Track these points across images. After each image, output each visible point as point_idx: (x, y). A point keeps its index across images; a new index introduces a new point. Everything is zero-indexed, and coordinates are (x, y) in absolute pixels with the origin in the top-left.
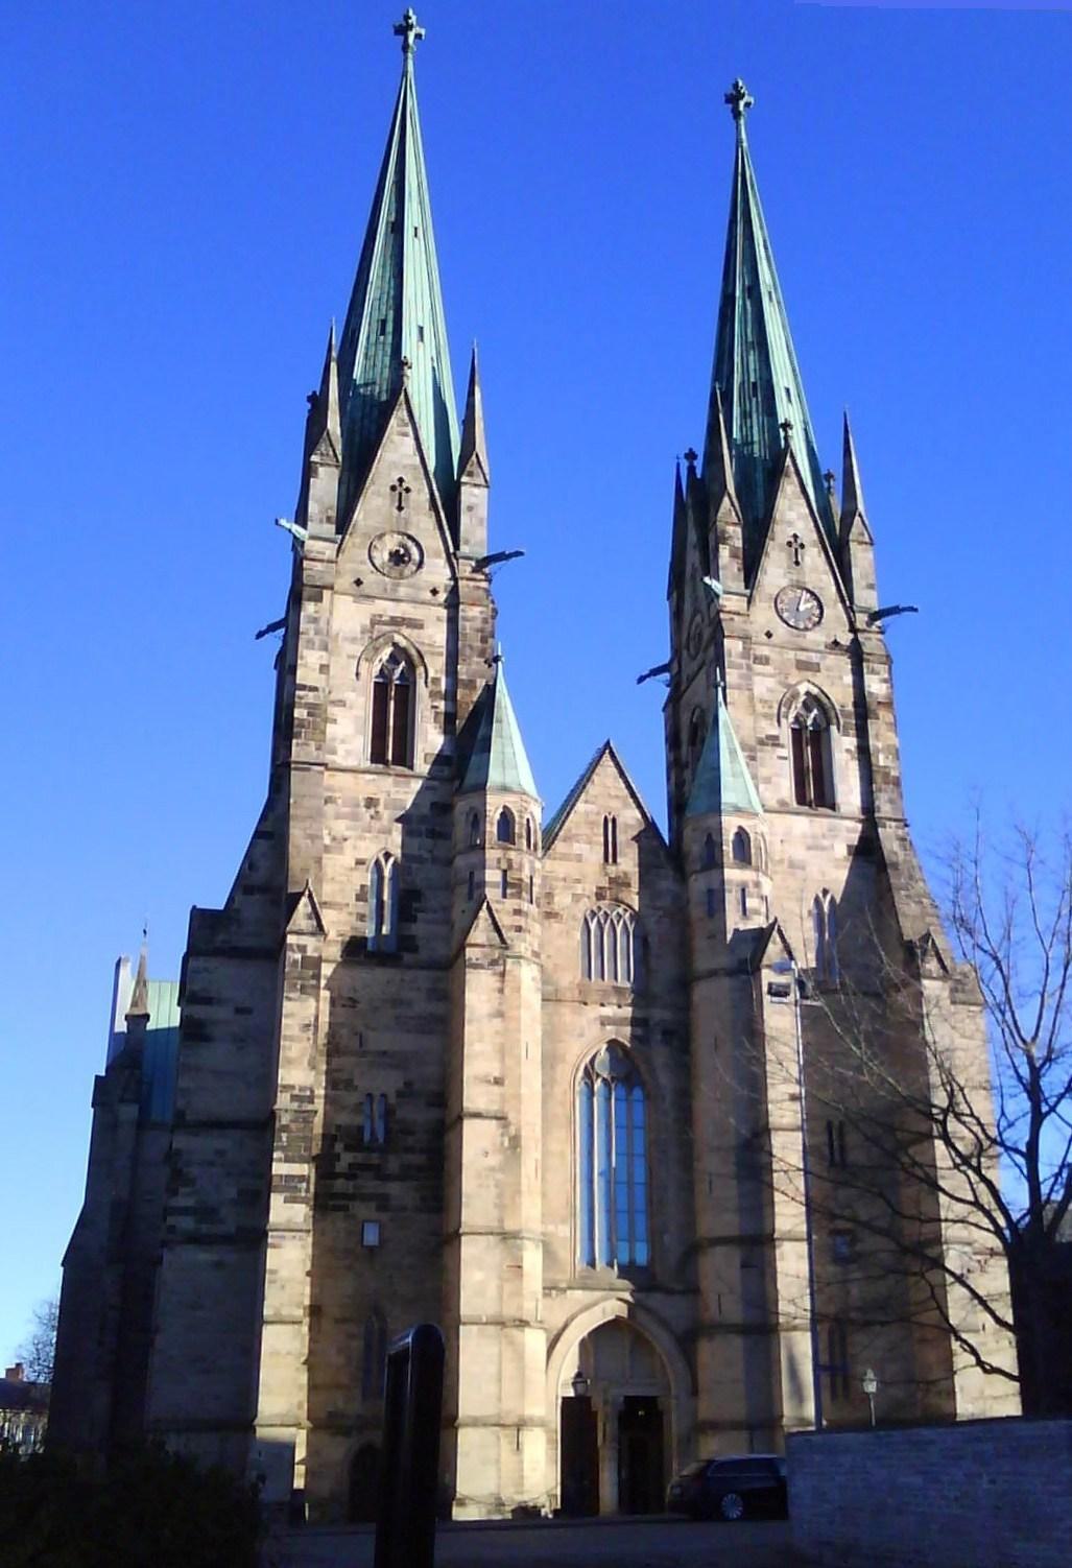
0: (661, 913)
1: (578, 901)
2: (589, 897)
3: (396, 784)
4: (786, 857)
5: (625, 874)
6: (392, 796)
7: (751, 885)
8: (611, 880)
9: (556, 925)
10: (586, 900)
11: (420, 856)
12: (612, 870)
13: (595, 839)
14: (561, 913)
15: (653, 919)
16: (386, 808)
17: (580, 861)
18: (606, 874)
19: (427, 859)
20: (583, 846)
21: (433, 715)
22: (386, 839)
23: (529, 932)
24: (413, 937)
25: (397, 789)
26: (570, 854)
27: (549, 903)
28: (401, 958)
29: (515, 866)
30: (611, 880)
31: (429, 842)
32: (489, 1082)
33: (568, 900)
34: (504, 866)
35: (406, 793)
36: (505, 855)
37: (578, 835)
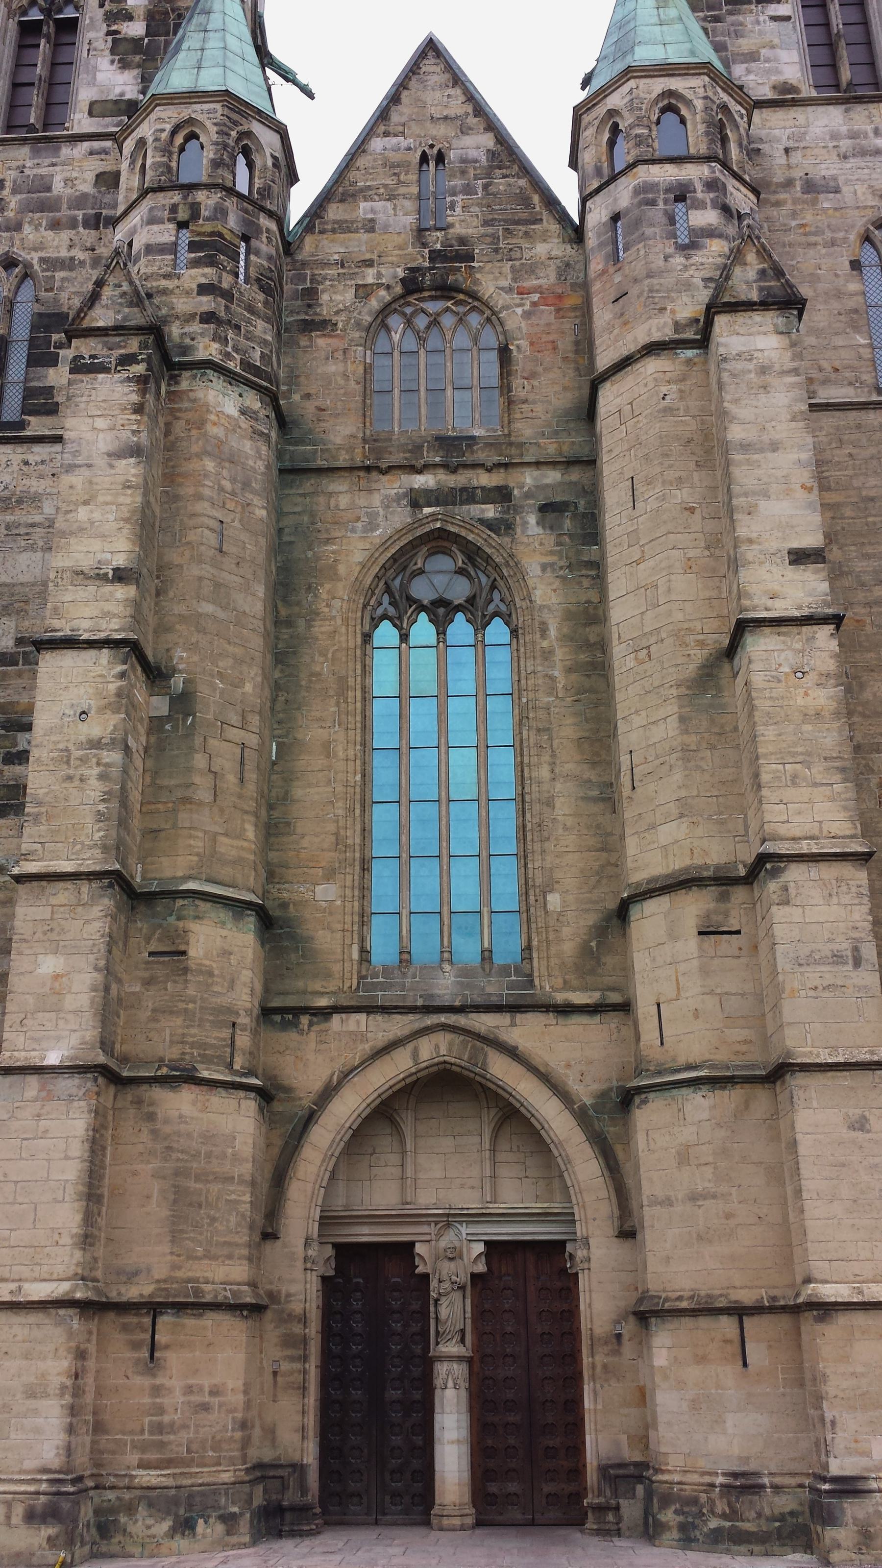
0: (535, 297)
1: (367, 296)
2: (388, 287)
3: (36, 153)
4: (797, 174)
5: (462, 241)
6: (27, 172)
7: (699, 187)
8: (434, 256)
9: (321, 342)
10: (383, 293)
11: (72, 259)
12: (437, 241)
13: (402, 190)
14: (334, 319)
15: (519, 311)
16: (14, 192)
17: (372, 230)
18: (424, 245)
19: (82, 263)
20: (379, 205)
21: (110, 44)
22: (12, 238)
23: (238, 327)
24: (49, 391)
25: (36, 161)
26: (352, 222)
27: (309, 306)
28: (21, 425)
29: (205, 213)
30: (434, 256)
31: (88, 236)
32: (104, 578)
33: (349, 296)
34: (183, 214)
35: (54, 165)
36: (185, 198)
37: (369, 188)
